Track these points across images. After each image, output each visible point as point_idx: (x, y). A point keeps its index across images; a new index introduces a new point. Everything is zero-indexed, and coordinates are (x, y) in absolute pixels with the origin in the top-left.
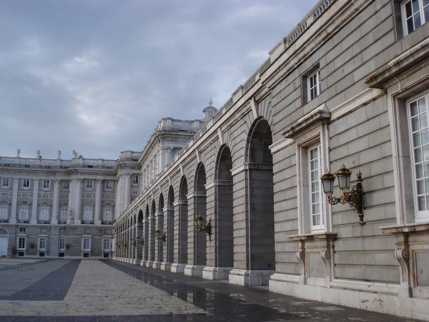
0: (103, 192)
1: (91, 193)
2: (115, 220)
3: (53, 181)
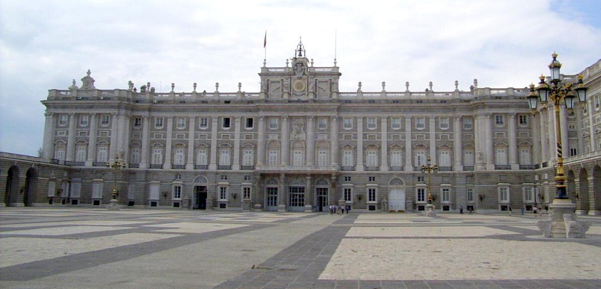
0: (517, 128)
1: (503, 130)
2: (545, 165)
3: (452, 120)
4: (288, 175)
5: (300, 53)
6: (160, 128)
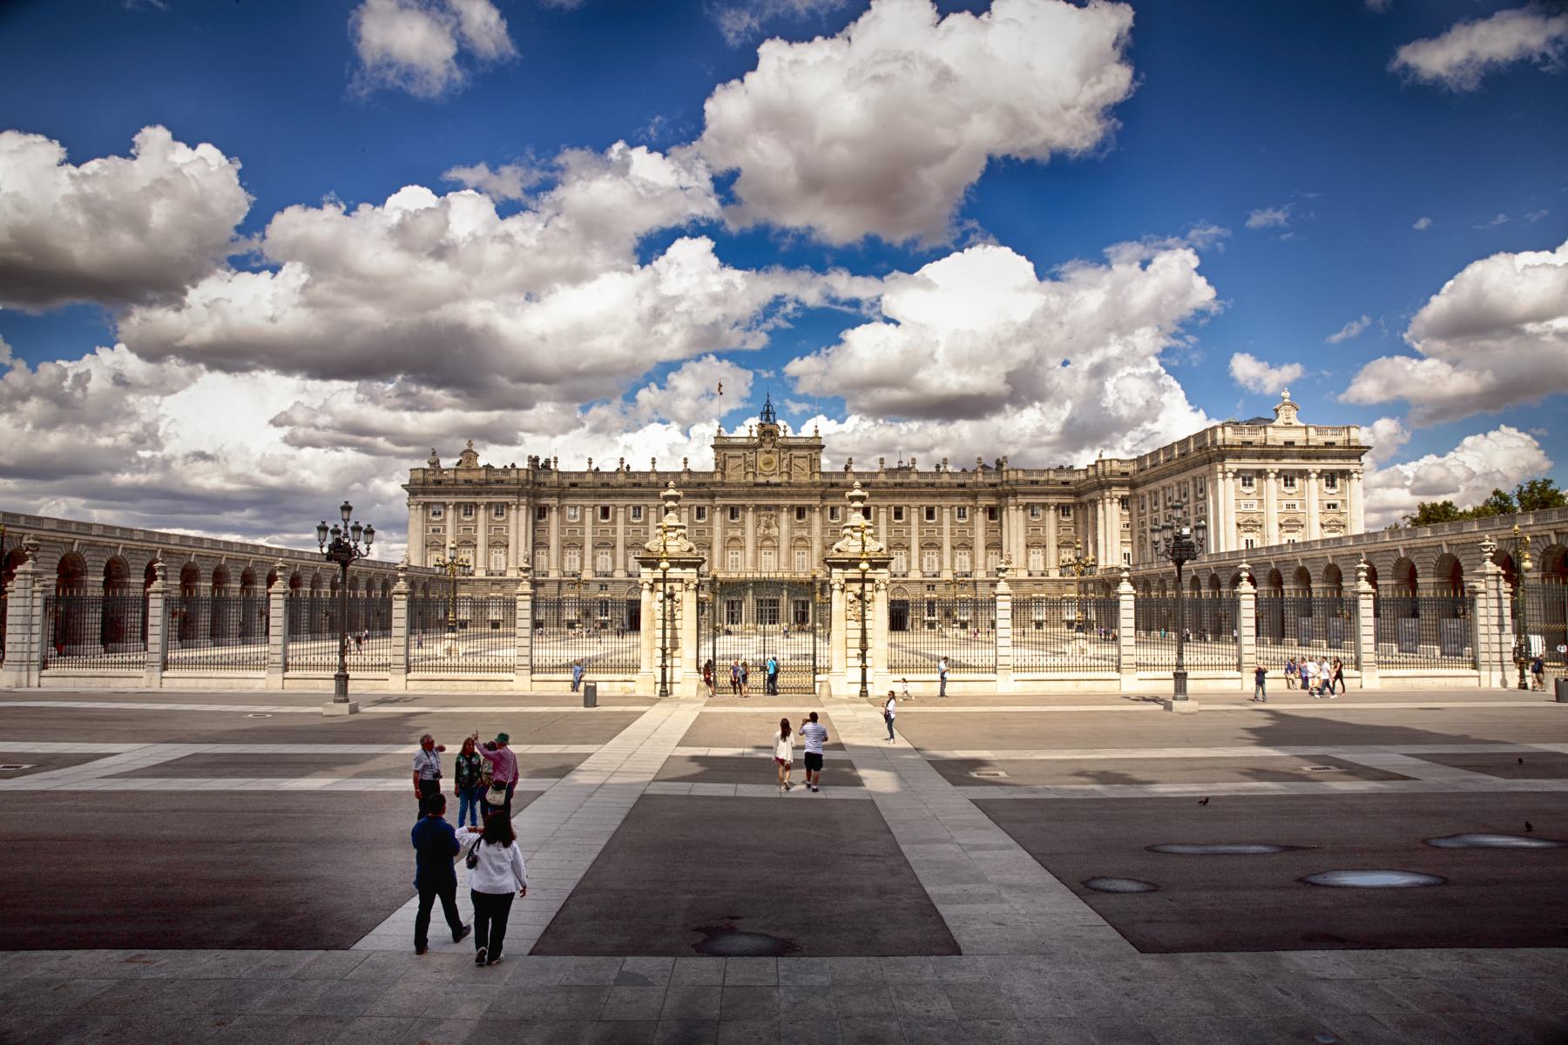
3: (974, 508)
4: (759, 584)
5: (768, 416)
6: (575, 521)
